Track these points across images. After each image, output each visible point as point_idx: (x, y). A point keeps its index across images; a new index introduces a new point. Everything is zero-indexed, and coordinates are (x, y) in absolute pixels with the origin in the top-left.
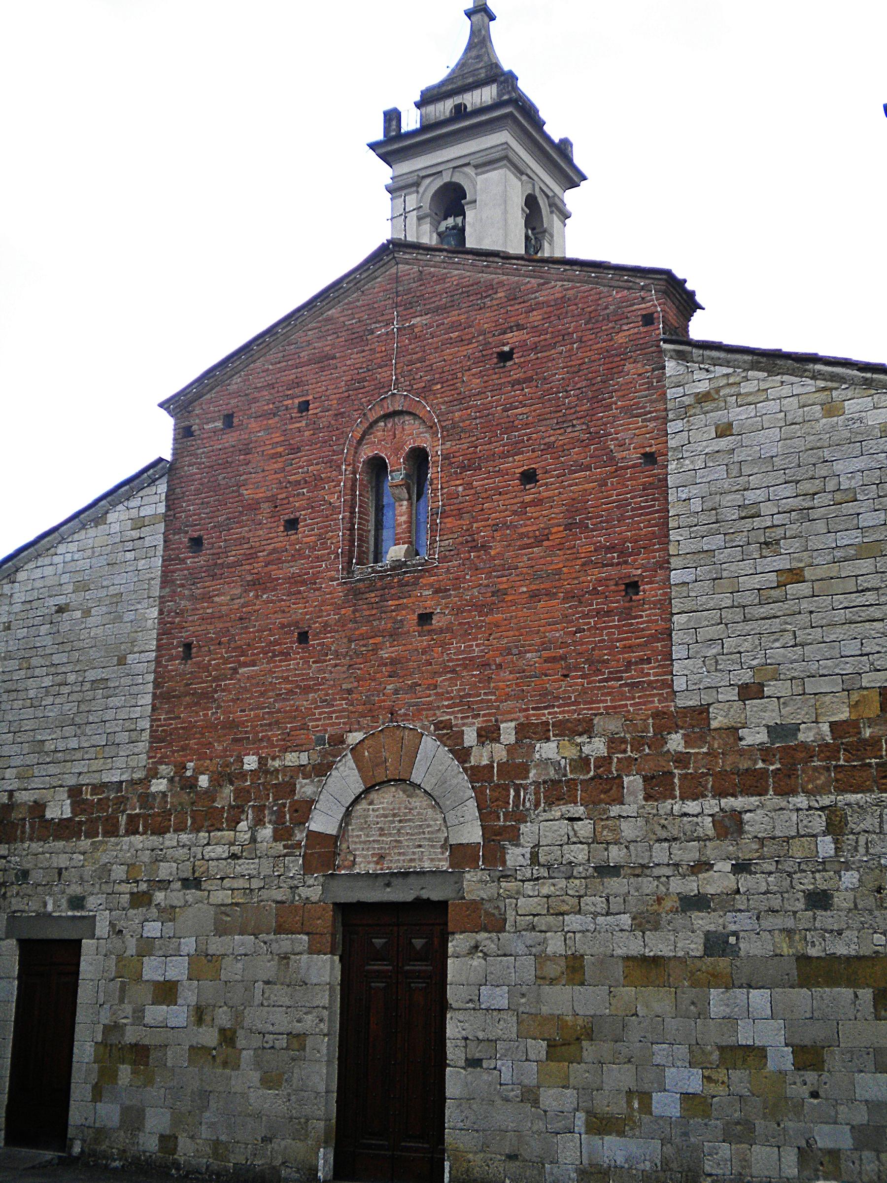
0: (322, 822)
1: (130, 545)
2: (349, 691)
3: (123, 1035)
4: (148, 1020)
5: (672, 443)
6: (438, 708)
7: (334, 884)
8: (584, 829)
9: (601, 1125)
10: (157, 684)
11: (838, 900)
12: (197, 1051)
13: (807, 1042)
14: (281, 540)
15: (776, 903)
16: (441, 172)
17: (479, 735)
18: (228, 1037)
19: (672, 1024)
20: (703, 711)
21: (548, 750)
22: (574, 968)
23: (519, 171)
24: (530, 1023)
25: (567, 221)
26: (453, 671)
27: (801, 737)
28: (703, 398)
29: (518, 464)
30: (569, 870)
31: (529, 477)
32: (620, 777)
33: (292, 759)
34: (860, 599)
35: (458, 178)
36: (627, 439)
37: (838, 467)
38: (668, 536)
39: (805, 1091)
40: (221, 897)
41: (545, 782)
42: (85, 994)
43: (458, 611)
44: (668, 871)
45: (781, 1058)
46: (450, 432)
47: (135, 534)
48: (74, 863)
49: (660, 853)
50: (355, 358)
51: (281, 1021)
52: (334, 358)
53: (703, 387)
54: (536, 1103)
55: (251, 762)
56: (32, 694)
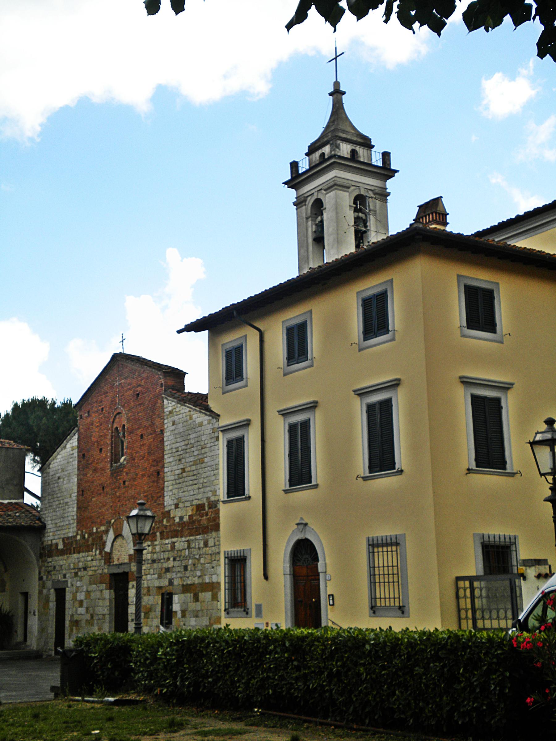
0: (107, 549)
2: (111, 506)
4: (79, 612)
10: (78, 504)
12: (87, 620)
16: (313, 194)
18: (92, 616)
20: (169, 512)
23: (345, 188)
25: (388, 198)
29: (139, 432)
31: (142, 436)
35: (321, 196)
40: (90, 573)
42: (67, 605)
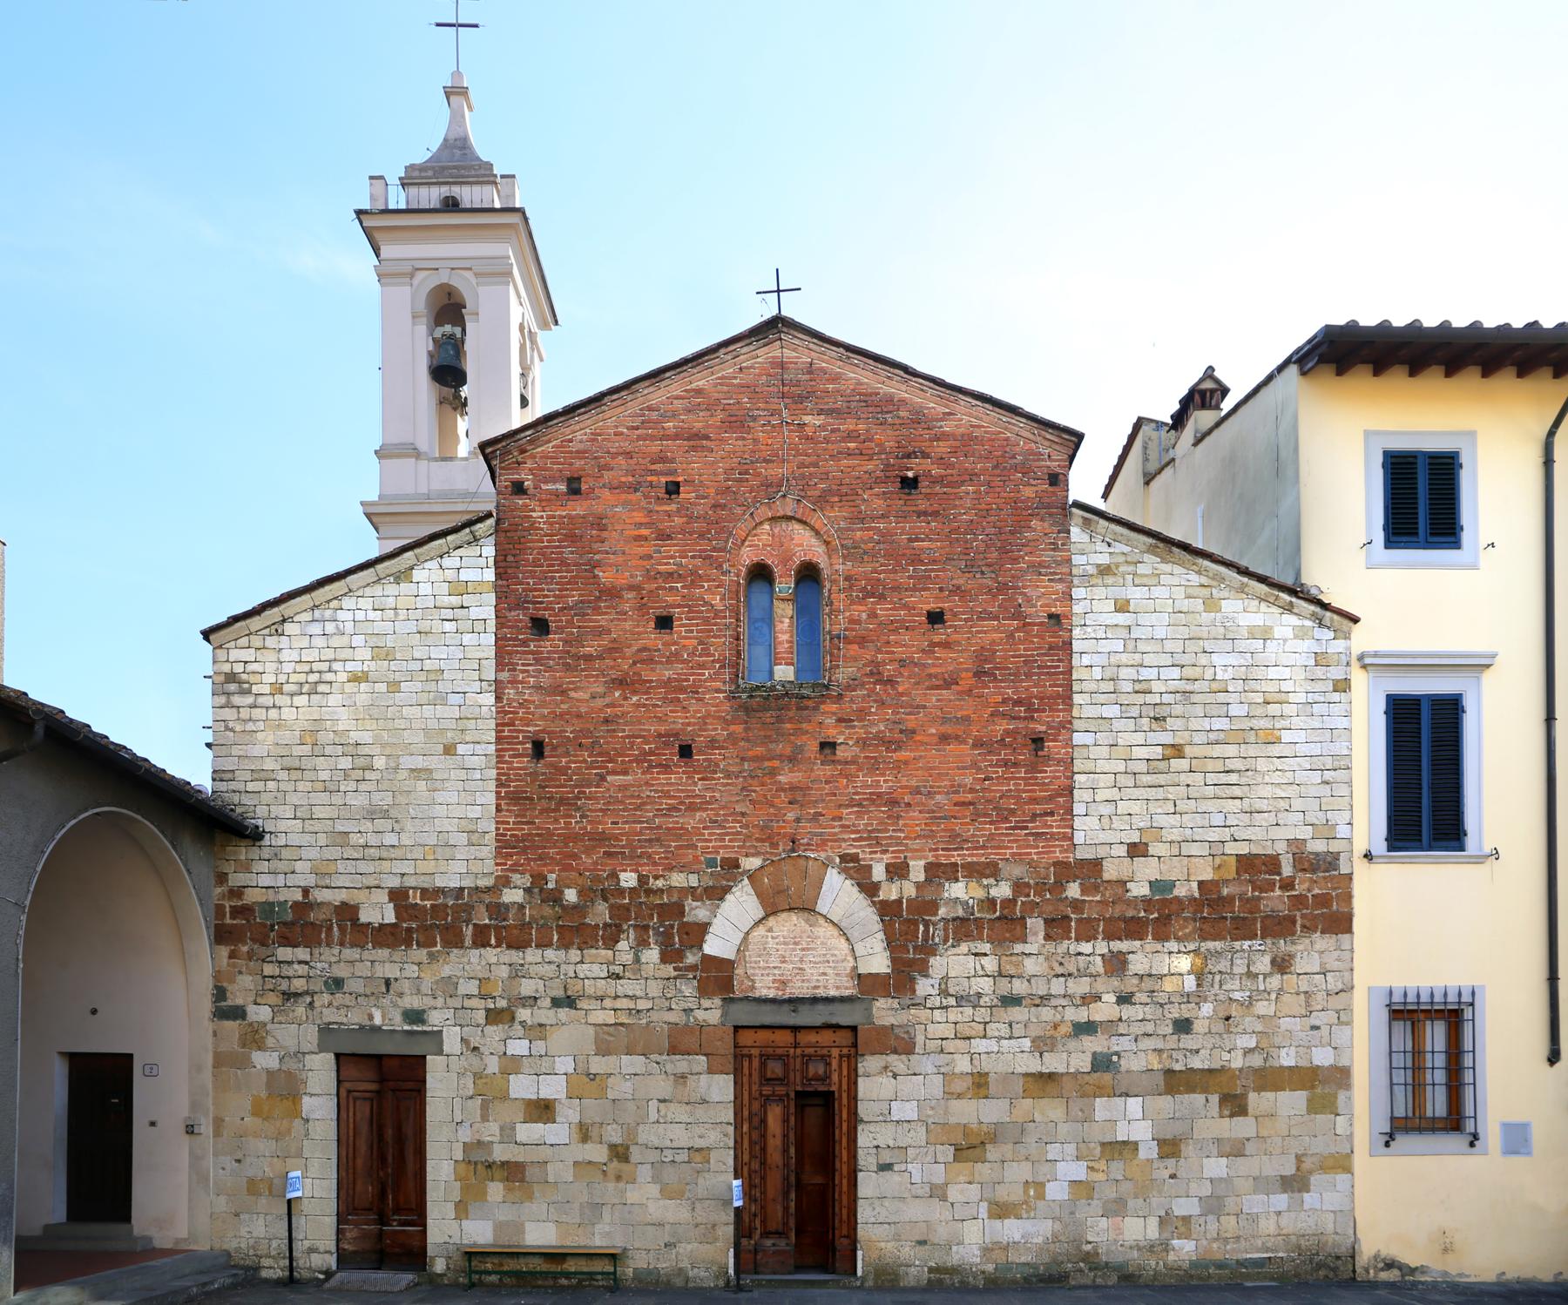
1: (449, 614)
3: (490, 1153)
5: (1077, 609)
6: (844, 840)
7: (734, 1007)
8: (990, 964)
9: (1001, 1211)
11: (1198, 1026)
13: (1168, 1137)
14: (653, 638)
15: (1150, 1028)
17: (887, 871)
18: (620, 1153)
19: (1064, 1129)
21: (957, 890)
22: (980, 1084)
24: (937, 1131)
26: (860, 805)
27: (1176, 892)
28: (1104, 571)
30: (973, 1000)
31: (935, 618)
32: (1023, 918)
33: (678, 879)
34: (1224, 778)
36: (1038, 597)
37: (1216, 659)
38: (1071, 698)
39: (1166, 1174)
41: (954, 919)
43: (863, 743)
44: (1064, 1002)
45: (1148, 1151)
46: (852, 552)
47: (455, 600)
48: (406, 974)
49: (1057, 986)
50: (733, 442)
51: (681, 1137)
52: (707, 438)
53: (1104, 559)
54: (944, 1198)
55: (628, 879)
56: (324, 775)
